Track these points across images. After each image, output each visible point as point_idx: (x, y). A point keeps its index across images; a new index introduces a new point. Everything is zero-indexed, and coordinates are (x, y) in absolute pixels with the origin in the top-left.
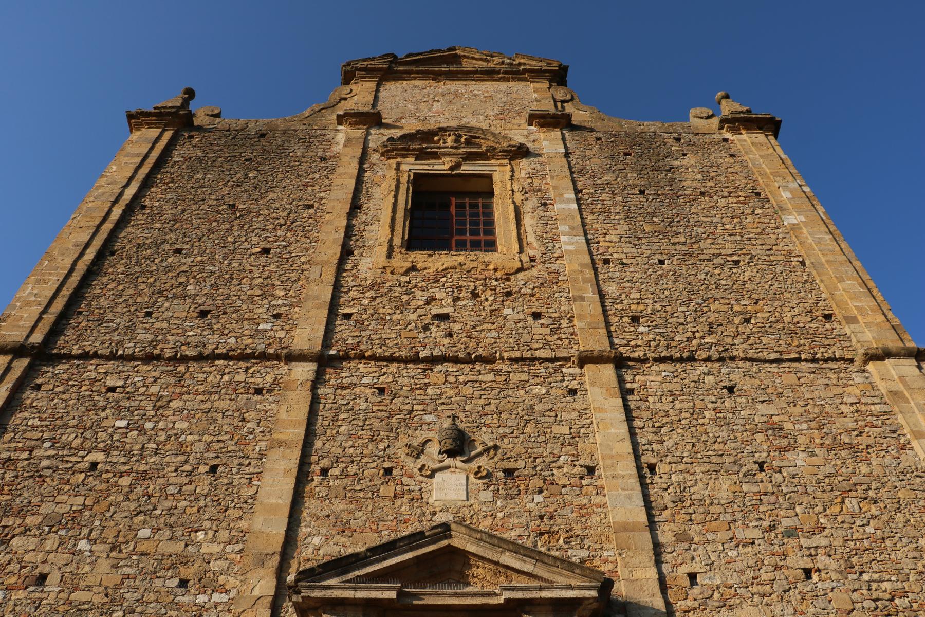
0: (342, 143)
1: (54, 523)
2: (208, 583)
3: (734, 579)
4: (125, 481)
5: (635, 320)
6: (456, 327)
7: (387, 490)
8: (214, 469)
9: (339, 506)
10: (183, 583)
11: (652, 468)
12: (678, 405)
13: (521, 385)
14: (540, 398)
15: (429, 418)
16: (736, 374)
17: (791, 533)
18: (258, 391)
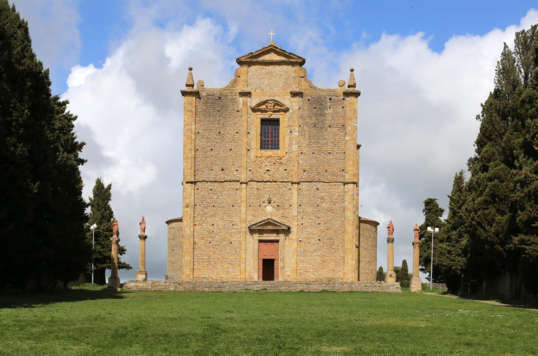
0: (242, 103)
2: (237, 225)
3: (308, 224)
4: (220, 208)
6: (270, 173)
7: (260, 209)
8: (233, 206)
9: (253, 212)
10: (233, 225)
12: (308, 193)
15: (266, 195)
17: (318, 218)
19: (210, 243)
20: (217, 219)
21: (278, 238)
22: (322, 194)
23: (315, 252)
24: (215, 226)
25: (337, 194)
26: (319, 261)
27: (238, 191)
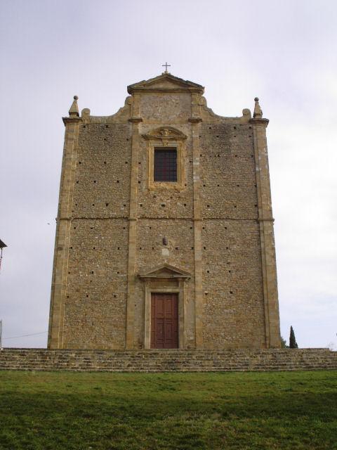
1: (91, 261)
2: (122, 273)
5: (208, 206)
7: (153, 253)
11: (205, 248)
13: (180, 226)
14: (184, 230)
16: (227, 223)
17: (228, 263)
18: (124, 228)
19: (87, 296)
20: (98, 266)
21: (177, 290)
22: (232, 234)
23: (226, 308)
24: (95, 274)
25: (250, 234)
26: (232, 321)
27: (126, 229)
